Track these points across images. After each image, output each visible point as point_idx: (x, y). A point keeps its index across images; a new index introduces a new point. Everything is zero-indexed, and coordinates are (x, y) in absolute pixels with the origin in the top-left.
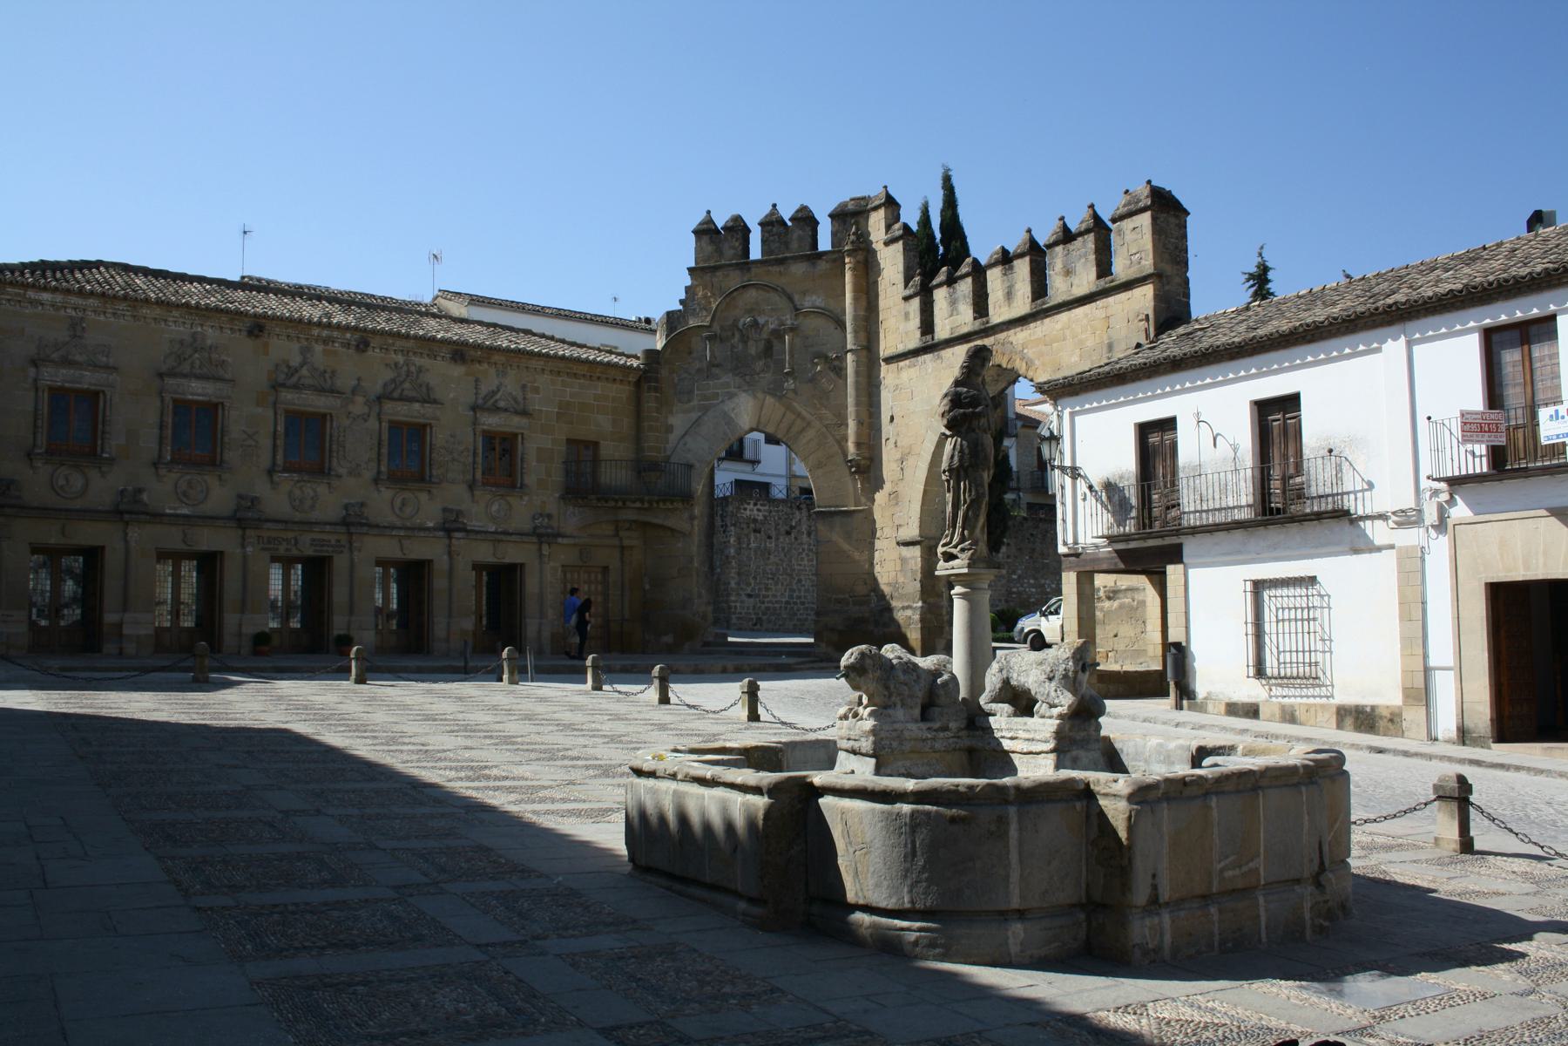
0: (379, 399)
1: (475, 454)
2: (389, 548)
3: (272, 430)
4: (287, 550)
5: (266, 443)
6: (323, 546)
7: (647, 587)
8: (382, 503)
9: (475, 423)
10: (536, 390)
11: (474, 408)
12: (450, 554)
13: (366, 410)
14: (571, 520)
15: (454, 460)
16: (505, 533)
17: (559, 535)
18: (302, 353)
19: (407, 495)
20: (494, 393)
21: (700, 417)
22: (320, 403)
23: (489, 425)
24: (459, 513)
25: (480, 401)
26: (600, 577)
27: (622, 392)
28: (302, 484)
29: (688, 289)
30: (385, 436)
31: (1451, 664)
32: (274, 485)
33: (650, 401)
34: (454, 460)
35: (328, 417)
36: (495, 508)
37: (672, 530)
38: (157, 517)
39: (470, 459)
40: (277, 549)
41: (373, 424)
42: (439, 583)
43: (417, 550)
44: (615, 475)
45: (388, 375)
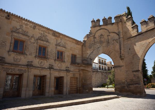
1: (56, 54)
2: (37, 72)
3: (10, 42)
4: (11, 71)
5: (8, 44)
6: (21, 71)
7: (83, 81)
8: (36, 62)
9: (56, 48)
10: (67, 44)
11: (56, 45)
12: (50, 74)
13: (34, 41)
14: (72, 68)
15: (52, 55)
16: (61, 70)
17: (70, 71)
18: (20, 26)
19: (42, 61)
20: (60, 43)
22: (23, 38)
23: (59, 49)
24: (52, 65)
25: (57, 44)
26: (76, 79)
27: (80, 47)
28: (17, 55)
29: (90, 31)
32: (10, 55)
33: (84, 49)
34: (52, 55)
35: (25, 41)
36: (59, 65)
37: (88, 71)
39: (55, 55)
40: (8, 71)
41: (35, 45)
42: (48, 80)
43: (43, 73)
44: (79, 60)
45: (40, 35)
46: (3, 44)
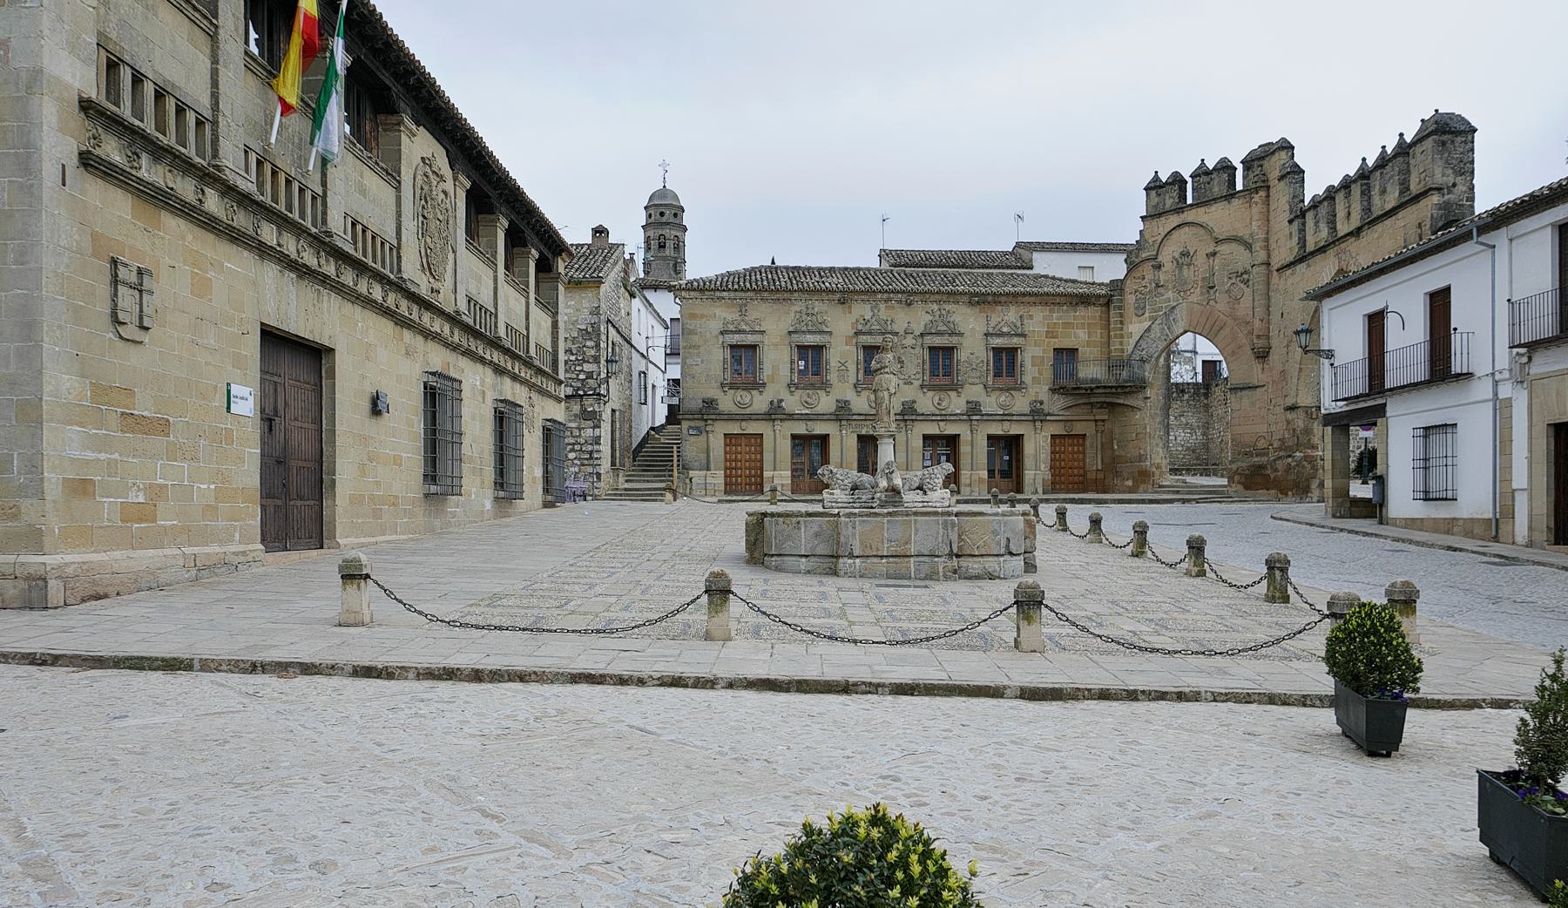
0: (922, 335)
5: (852, 368)
7: (1116, 447)
21: (1150, 326)
24: (977, 404)
30: (927, 357)
31: (1526, 487)
38: (791, 417)
41: (918, 350)
46: (843, 368)
